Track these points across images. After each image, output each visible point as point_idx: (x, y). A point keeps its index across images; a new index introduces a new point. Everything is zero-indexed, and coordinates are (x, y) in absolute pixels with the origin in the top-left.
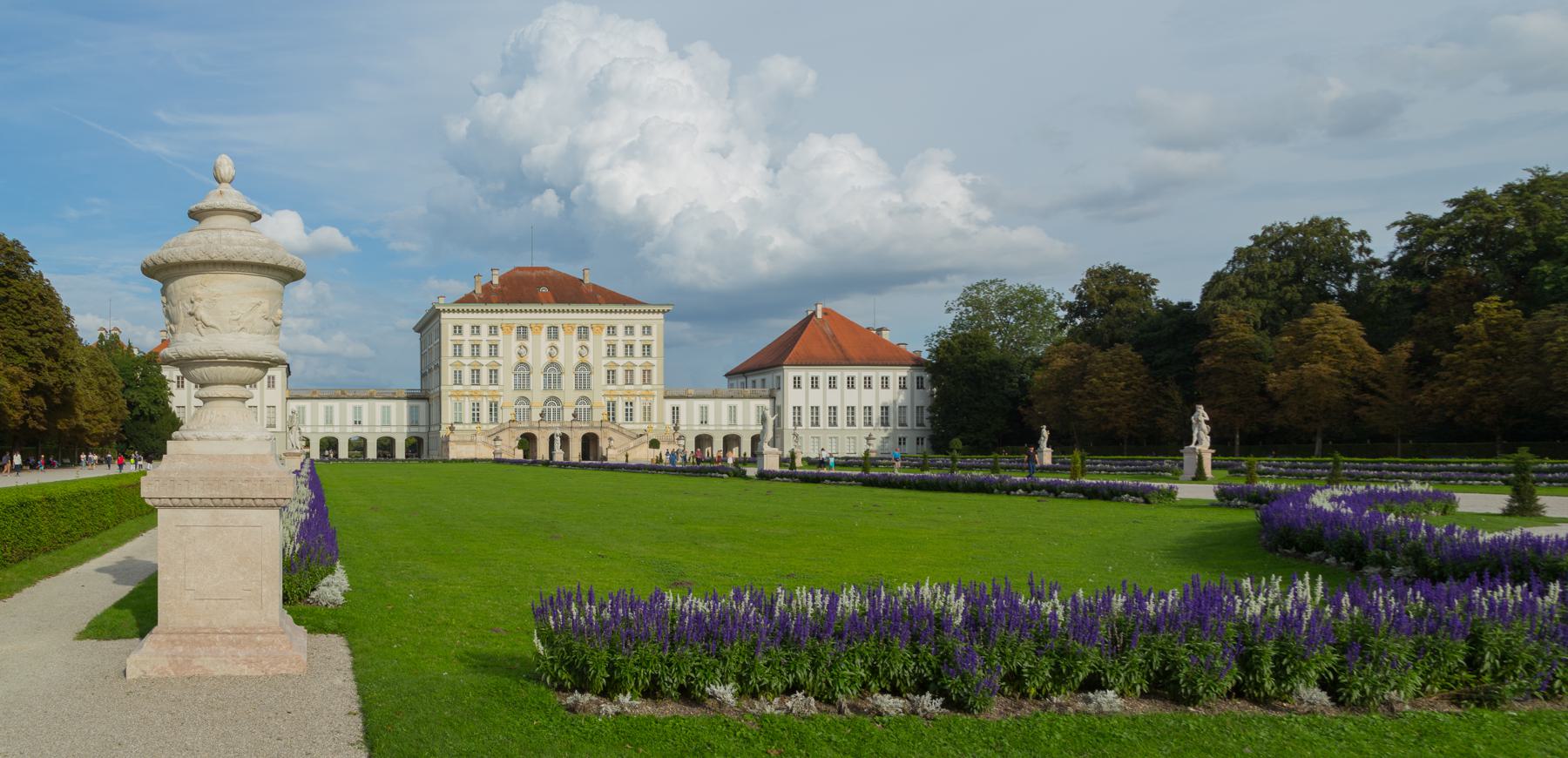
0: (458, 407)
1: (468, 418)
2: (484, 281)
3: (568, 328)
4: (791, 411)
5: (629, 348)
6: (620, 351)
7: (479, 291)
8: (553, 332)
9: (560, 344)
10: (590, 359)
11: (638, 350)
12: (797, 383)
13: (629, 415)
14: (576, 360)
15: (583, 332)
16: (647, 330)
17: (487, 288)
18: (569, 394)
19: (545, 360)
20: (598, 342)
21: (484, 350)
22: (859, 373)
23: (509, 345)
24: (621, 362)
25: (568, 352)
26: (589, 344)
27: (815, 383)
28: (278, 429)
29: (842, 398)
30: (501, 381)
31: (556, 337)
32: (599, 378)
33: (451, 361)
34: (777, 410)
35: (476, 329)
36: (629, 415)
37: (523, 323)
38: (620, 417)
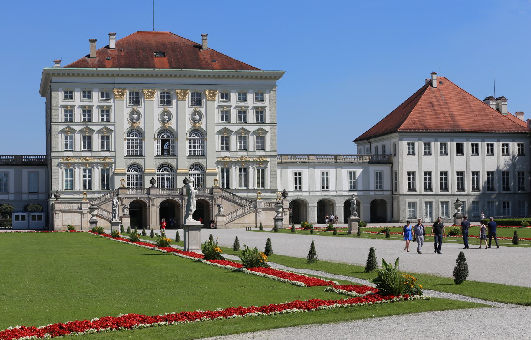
1: (79, 186)
4: (406, 177)
5: (243, 114)
6: (234, 116)
7: (93, 55)
9: (173, 110)
11: (251, 116)
14: (189, 126)
16: (260, 97)
18: (183, 161)
19: (157, 126)
26: (203, 110)
31: (169, 103)
32: (214, 143)
33: (61, 128)
34: (394, 177)
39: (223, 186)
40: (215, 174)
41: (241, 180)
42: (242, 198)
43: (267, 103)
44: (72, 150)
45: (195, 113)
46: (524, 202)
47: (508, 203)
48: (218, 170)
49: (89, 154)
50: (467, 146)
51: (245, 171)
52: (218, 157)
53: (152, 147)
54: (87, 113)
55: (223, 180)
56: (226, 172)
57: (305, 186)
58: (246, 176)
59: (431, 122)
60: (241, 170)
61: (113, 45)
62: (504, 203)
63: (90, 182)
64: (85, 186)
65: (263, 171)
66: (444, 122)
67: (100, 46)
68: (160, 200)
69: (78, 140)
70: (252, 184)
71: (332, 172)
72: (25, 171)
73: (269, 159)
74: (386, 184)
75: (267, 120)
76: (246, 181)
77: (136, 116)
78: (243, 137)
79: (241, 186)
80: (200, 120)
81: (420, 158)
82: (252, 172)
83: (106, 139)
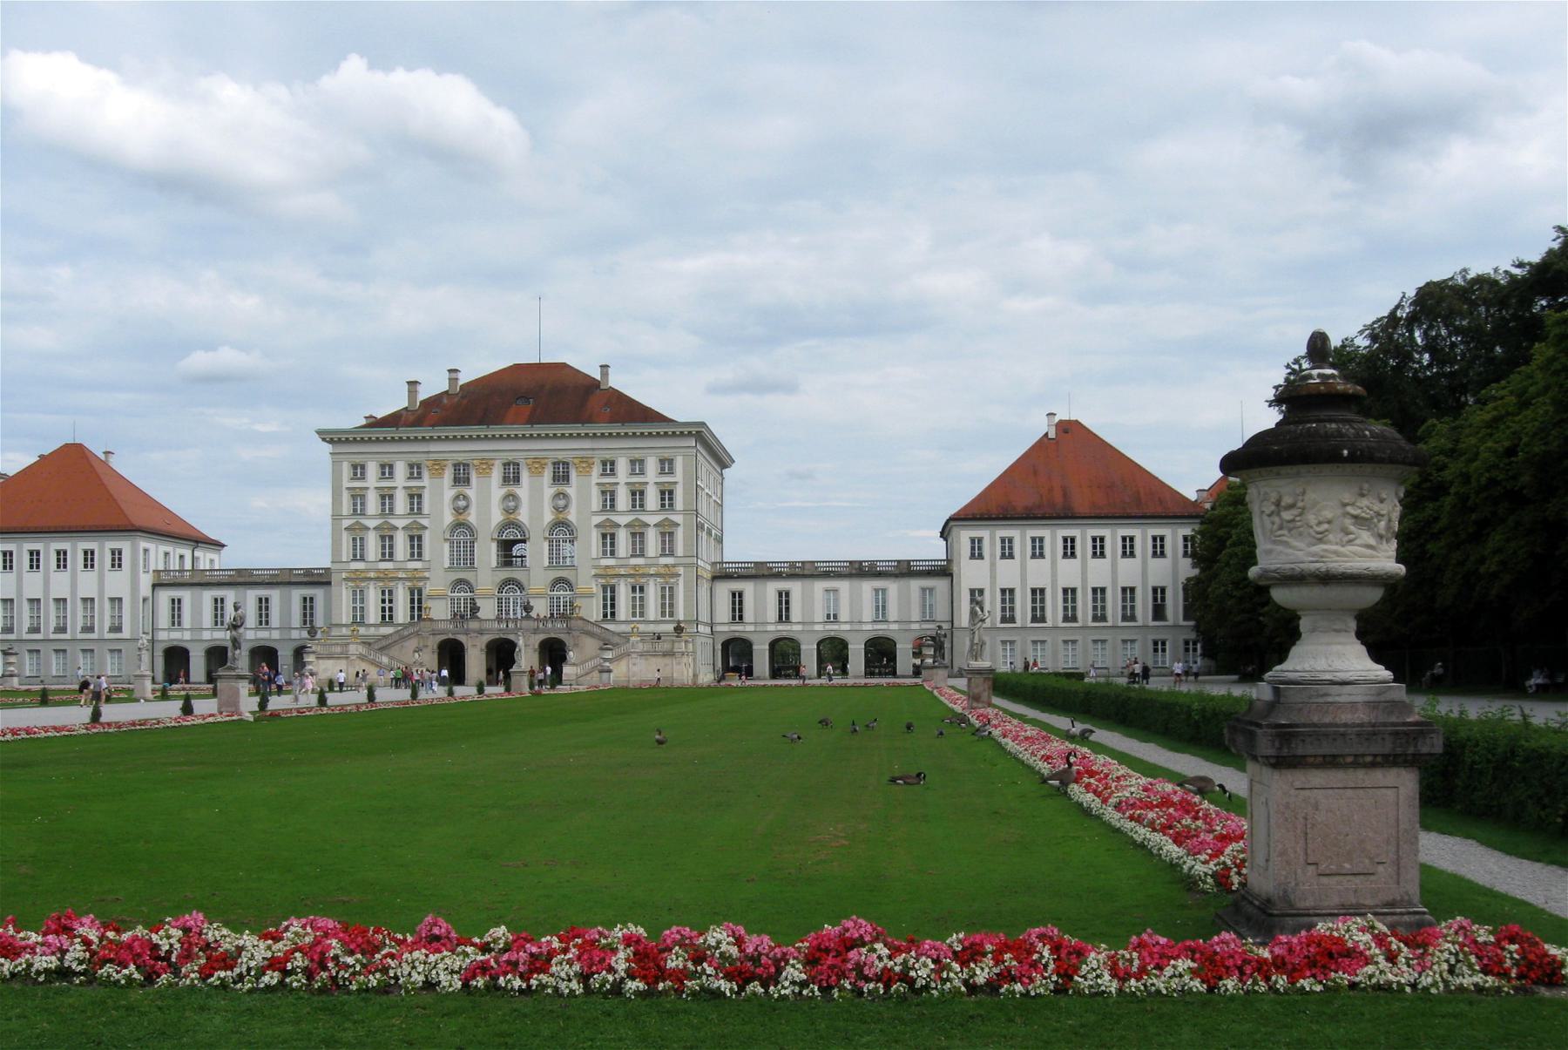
0: (359, 596)
1: (373, 615)
2: (424, 394)
3: (537, 465)
5: (637, 495)
6: (623, 500)
8: (512, 476)
9: (523, 491)
10: (572, 516)
11: (652, 499)
12: (977, 554)
13: (639, 607)
14: (549, 517)
15: (561, 475)
16: (666, 465)
19: (497, 517)
21: (401, 504)
22: (1083, 535)
23: (440, 494)
24: (623, 520)
25: (535, 501)
26: (571, 491)
27: (1038, 552)
28: (126, 634)
30: (427, 555)
31: (517, 480)
33: (346, 523)
35: (387, 470)
36: (639, 607)
37: (461, 458)
39: (605, 615)
40: (591, 596)
41: (634, 607)
42: (619, 634)
43: (679, 476)
44: (362, 559)
45: (558, 495)
46: (1195, 643)
47: (1164, 643)
48: (595, 588)
49: (389, 565)
51: (642, 589)
52: (595, 567)
53: (487, 553)
54: (387, 497)
55: (605, 606)
57: (796, 614)
58: (642, 599)
60: (634, 589)
62: (1156, 643)
63: (391, 609)
64: (383, 617)
65: (671, 589)
68: (487, 638)
70: (652, 611)
73: (681, 570)
76: (642, 606)
77: (462, 503)
79: (634, 614)
80: (566, 506)
81: (993, 565)
83: (416, 541)
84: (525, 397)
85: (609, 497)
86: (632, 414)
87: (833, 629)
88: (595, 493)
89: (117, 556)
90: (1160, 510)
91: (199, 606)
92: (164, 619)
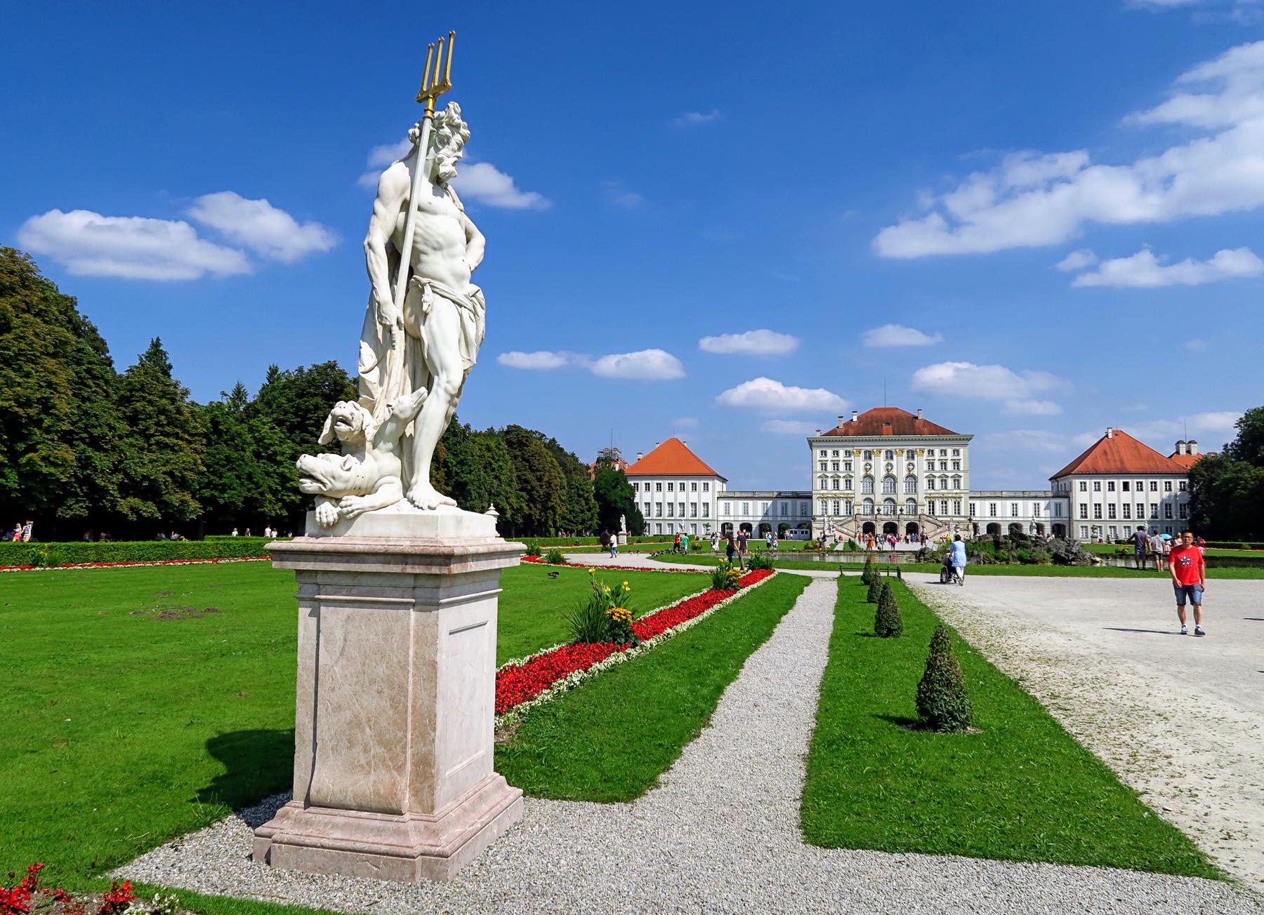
0: (825, 503)
1: (831, 512)
5: (944, 464)
6: (937, 466)
8: (890, 455)
9: (894, 462)
11: (950, 466)
14: (905, 473)
15: (911, 455)
16: (956, 452)
17: (848, 425)
19: (884, 473)
20: (921, 463)
21: (842, 466)
23: (859, 463)
26: (915, 462)
28: (710, 517)
29: (1119, 497)
32: (923, 484)
38: (938, 511)
43: (961, 456)
50: (1133, 483)
54: (836, 465)
56: (932, 504)
57: (999, 514)
59: (1102, 466)
61: (855, 419)
66: (1113, 466)
67: (845, 420)
69: (830, 482)
70: (951, 511)
71: (1020, 503)
72: (799, 502)
74: (1065, 512)
75: (962, 468)
78: (944, 481)
82: (951, 504)
84: (888, 424)
85: (931, 464)
86: (938, 432)
87: (1015, 520)
88: (926, 463)
89: (706, 486)
90: (1168, 470)
91: (737, 508)
92: (722, 511)
